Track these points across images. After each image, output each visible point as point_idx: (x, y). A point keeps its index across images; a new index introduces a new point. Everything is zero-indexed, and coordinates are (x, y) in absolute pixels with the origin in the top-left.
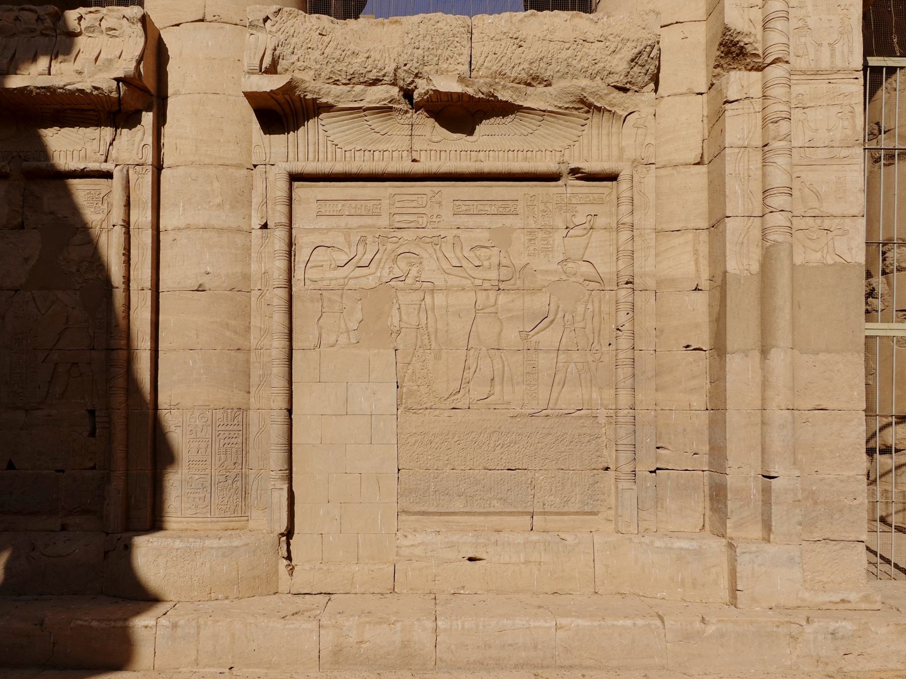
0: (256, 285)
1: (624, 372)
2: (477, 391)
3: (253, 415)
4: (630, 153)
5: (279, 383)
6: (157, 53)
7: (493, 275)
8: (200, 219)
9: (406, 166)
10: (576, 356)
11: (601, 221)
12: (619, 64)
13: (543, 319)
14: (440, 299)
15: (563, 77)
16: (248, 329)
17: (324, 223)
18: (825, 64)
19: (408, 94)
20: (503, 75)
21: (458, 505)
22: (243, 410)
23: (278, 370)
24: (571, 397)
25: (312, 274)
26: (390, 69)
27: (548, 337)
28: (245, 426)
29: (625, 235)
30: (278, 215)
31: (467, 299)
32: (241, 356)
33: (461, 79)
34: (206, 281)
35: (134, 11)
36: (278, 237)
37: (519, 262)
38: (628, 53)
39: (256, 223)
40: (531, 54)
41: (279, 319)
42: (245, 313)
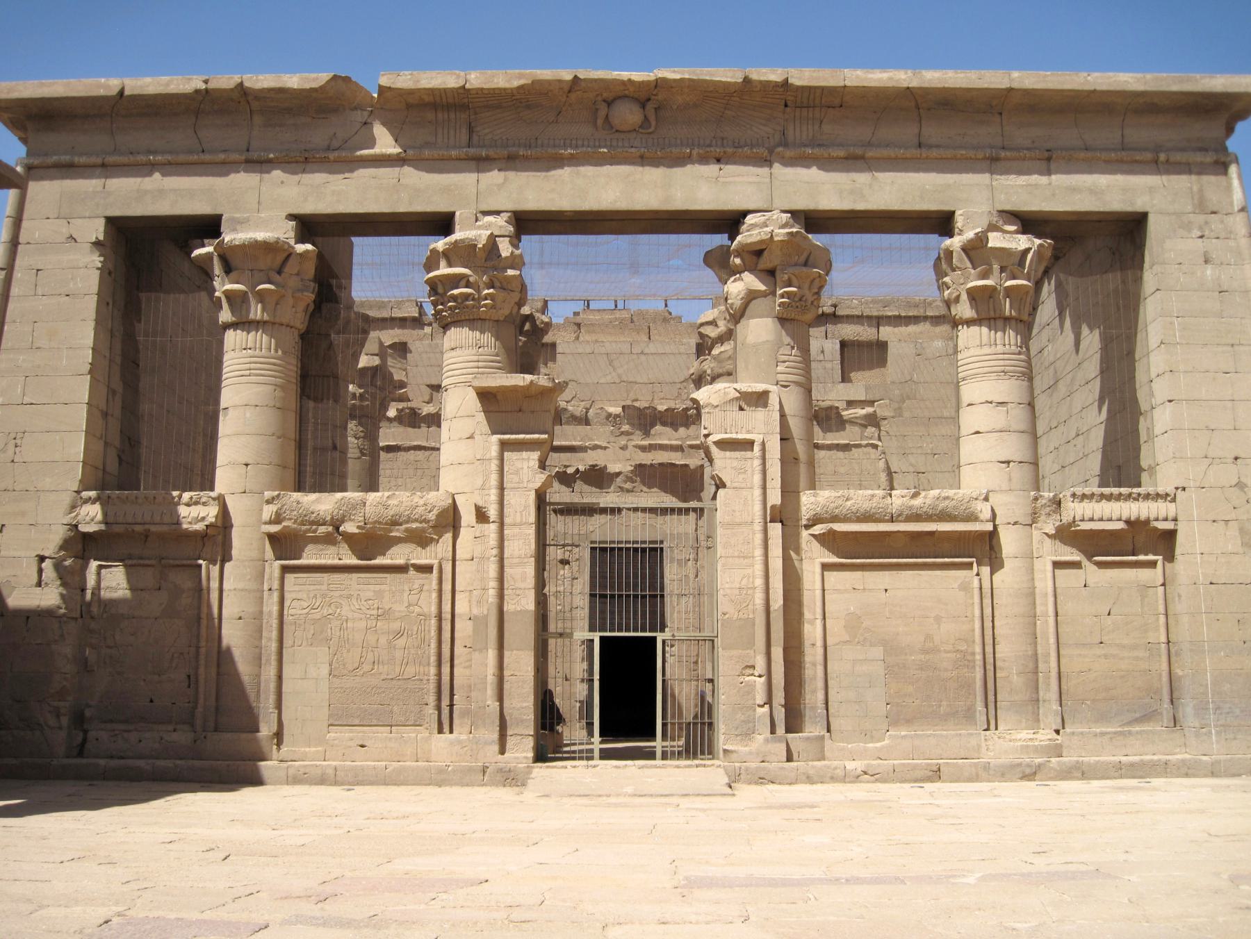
0: (265, 617)
1: (433, 659)
2: (366, 667)
3: (263, 678)
4: (440, 556)
5: (274, 663)
6: (224, 513)
7: (375, 612)
8: (241, 586)
9: (336, 562)
10: (413, 651)
11: (425, 588)
12: (432, 516)
13: (399, 634)
14: (350, 624)
15: (407, 522)
16: (261, 637)
17: (297, 588)
18: (518, 520)
19: (337, 529)
20: (380, 523)
21: (357, 722)
22: (259, 676)
23: (274, 657)
24: (410, 671)
25: (291, 611)
26: (328, 518)
27: (401, 642)
28: (259, 684)
29: (434, 595)
30: (276, 585)
31: (363, 624)
32: (257, 650)
33: (358, 527)
34: (242, 614)
35: (213, 494)
36: (276, 595)
37: (387, 607)
38: (435, 512)
39: (266, 587)
40: (392, 513)
41: (274, 634)
42: (260, 631)
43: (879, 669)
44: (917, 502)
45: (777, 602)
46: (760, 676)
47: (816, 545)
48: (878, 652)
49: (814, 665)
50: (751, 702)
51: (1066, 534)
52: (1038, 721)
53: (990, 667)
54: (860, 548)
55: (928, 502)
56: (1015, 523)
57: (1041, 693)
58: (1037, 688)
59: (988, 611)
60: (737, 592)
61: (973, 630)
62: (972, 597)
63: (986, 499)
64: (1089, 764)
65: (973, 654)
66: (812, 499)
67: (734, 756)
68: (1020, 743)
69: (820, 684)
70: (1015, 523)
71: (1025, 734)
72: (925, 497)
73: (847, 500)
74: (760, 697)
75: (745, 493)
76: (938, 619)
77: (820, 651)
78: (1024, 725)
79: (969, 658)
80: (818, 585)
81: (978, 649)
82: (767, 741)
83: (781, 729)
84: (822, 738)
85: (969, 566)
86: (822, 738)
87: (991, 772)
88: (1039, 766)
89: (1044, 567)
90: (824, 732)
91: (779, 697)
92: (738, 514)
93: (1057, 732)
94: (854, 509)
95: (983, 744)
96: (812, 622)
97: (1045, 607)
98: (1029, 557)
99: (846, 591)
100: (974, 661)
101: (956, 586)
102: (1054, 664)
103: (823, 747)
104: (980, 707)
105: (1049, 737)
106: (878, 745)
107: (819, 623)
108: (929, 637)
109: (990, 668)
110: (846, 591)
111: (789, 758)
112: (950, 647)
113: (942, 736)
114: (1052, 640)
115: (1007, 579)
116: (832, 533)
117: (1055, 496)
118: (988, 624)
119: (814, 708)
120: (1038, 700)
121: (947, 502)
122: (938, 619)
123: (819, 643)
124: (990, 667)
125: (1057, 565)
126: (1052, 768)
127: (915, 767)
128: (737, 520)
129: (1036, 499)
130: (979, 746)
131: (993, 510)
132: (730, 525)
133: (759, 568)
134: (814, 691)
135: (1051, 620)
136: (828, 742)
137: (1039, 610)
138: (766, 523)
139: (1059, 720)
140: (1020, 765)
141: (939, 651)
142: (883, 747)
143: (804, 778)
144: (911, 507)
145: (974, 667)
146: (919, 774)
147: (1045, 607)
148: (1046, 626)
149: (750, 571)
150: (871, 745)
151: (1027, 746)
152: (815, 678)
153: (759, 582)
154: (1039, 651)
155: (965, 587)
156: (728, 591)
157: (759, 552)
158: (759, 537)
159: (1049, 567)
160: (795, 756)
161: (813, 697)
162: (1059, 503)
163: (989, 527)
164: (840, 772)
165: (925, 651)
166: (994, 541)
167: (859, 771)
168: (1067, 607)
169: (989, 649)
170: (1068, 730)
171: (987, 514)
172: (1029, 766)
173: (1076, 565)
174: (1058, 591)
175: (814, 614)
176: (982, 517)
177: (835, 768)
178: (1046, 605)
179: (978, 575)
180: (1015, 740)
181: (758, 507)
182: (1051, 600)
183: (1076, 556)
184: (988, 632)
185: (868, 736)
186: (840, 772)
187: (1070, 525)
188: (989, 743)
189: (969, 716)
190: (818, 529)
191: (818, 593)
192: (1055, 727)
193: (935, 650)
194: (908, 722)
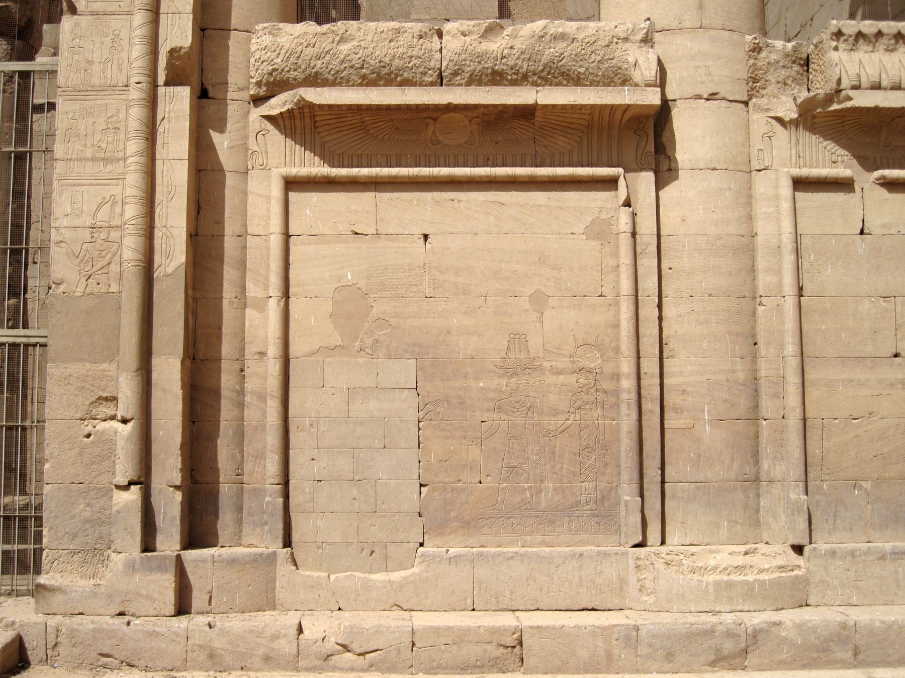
43: (405, 407)
44: (495, 46)
45: (173, 255)
46: (125, 421)
47: (275, 137)
48: (404, 372)
49: (262, 398)
50: (104, 479)
51: (825, 119)
52: (757, 524)
53: (651, 407)
54: (370, 141)
55: (519, 44)
56: (712, 96)
57: (765, 465)
58: (756, 455)
59: (649, 284)
60: (87, 235)
61: (617, 326)
62: (616, 254)
63: (647, 40)
64: (871, 631)
65: (616, 377)
66: (267, 40)
67: (58, 599)
68: (713, 578)
69: (272, 440)
70: (712, 96)
71: (725, 556)
72: (513, 36)
73: (343, 40)
74: (124, 467)
75: (116, 23)
76: (539, 301)
77: (274, 367)
78: (724, 533)
79: (607, 385)
80: (276, 224)
81: (627, 366)
82: (131, 567)
83: (169, 540)
84: (271, 559)
85: (611, 183)
86: (271, 559)
87: (643, 650)
88: (755, 636)
89: (773, 189)
90: (276, 546)
91: (169, 468)
92: (96, 68)
93: (798, 549)
94: (355, 59)
95: (632, 579)
96: (261, 306)
97: (776, 276)
98: (746, 170)
99: (338, 237)
100: (617, 393)
101: (580, 228)
102: (793, 400)
103: (274, 581)
104: (628, 495)
105: (780, 561)
106: (397, 576)
107: (274, 309)
108: (517, 339)
109: (653, 409)
110: (338, 237)
111: (182, 608)
112: (564, 363)
113: (539, 557)
114: (791, 348)
115: (691, 204)
116: (305, 109)
117: (795, 50)
118: (649, 312)
119: (259, 493)
120: (757, 479)
121: (561, 46)
122: (539, 301)
123: (273, 350)
124: (651, 407)
125: (800, 184)
126: (784, 640)
127: (461, 636)
128: (96, 81)
129: (757, 49)
130: (623, 582)
131: (660, 63)
132: (83, 91)
133: (133, 182)
134: (260, 456)
135: (790, 303)
136: (283, 569)
137: (764, 280)
138: (155, 86)
139: (803, 524)
140: (710, 632)
141: (540, 369)
142: (401, 586)
143: (203, 657)
144: (480, 57)
145: (616, 405)
146: (470, 651)
147: (776, 276)
148: (778, 317)
149: (117, 191)
150: (378, 577)
151: (730, 585)
152: (261, 427)
153: (132, 211)
154: (763, 373)
155: (599, 231)
156: (68, 235)
157: (134, 146)
158: (136, 115)
159: (786, 188)
160: (198, 600)
161: (247, 465)
162: (807, 62)
163: (653, 98)
164: (287, 646)
165: (508, 370)
166: (666, 134)
167: (331, 644)
168: (825, 278)
169: (650, 366)
170: (821, 545)
171: (647, 70)
172: (730, 634)
173: (843, 185)
174: (806, 242)
175: (266, 287)
176: (637, 76)
177: (275, 637)
178: (779, 272)
179: (627, 204)
180: (705, 569)
181: (138, 50)
182: (789, 259)
183: (842, 165)
184: (649, 331)
185: (376, 555)
186: (287, 646)
187: (829, 99)
188: (647, 575)
189: (603, 513)
190: (278, 105)
191: (276, 241)
192: (796, 542)
193: (530, 368)
194: (469, 525)
